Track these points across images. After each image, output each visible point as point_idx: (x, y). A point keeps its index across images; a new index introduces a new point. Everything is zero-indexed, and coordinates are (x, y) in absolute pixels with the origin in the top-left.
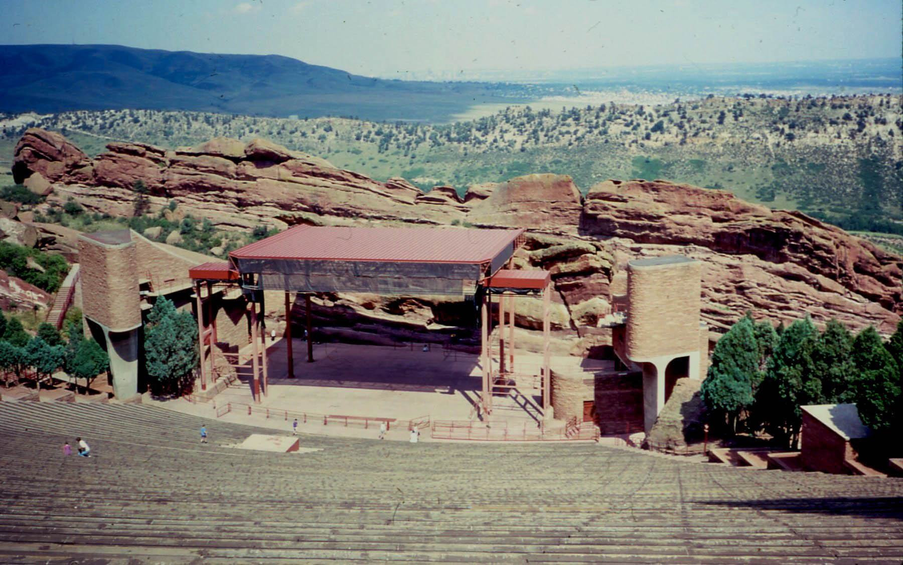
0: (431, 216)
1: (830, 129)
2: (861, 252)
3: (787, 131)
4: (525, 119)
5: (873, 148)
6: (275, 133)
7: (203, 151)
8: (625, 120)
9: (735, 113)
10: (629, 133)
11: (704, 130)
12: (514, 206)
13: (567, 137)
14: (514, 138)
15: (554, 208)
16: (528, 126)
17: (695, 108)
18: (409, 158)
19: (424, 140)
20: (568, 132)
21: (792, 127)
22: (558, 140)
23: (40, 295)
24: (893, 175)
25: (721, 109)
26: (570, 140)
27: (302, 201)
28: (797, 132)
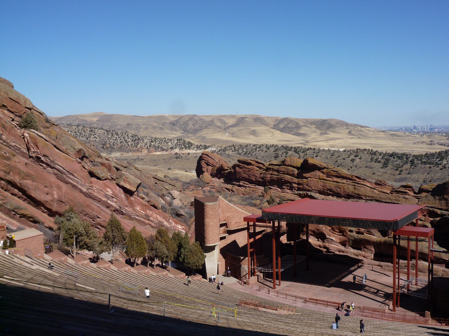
6: (329, 157)
18: (398, 172)
19: (407, 163)
23: (183, 227)
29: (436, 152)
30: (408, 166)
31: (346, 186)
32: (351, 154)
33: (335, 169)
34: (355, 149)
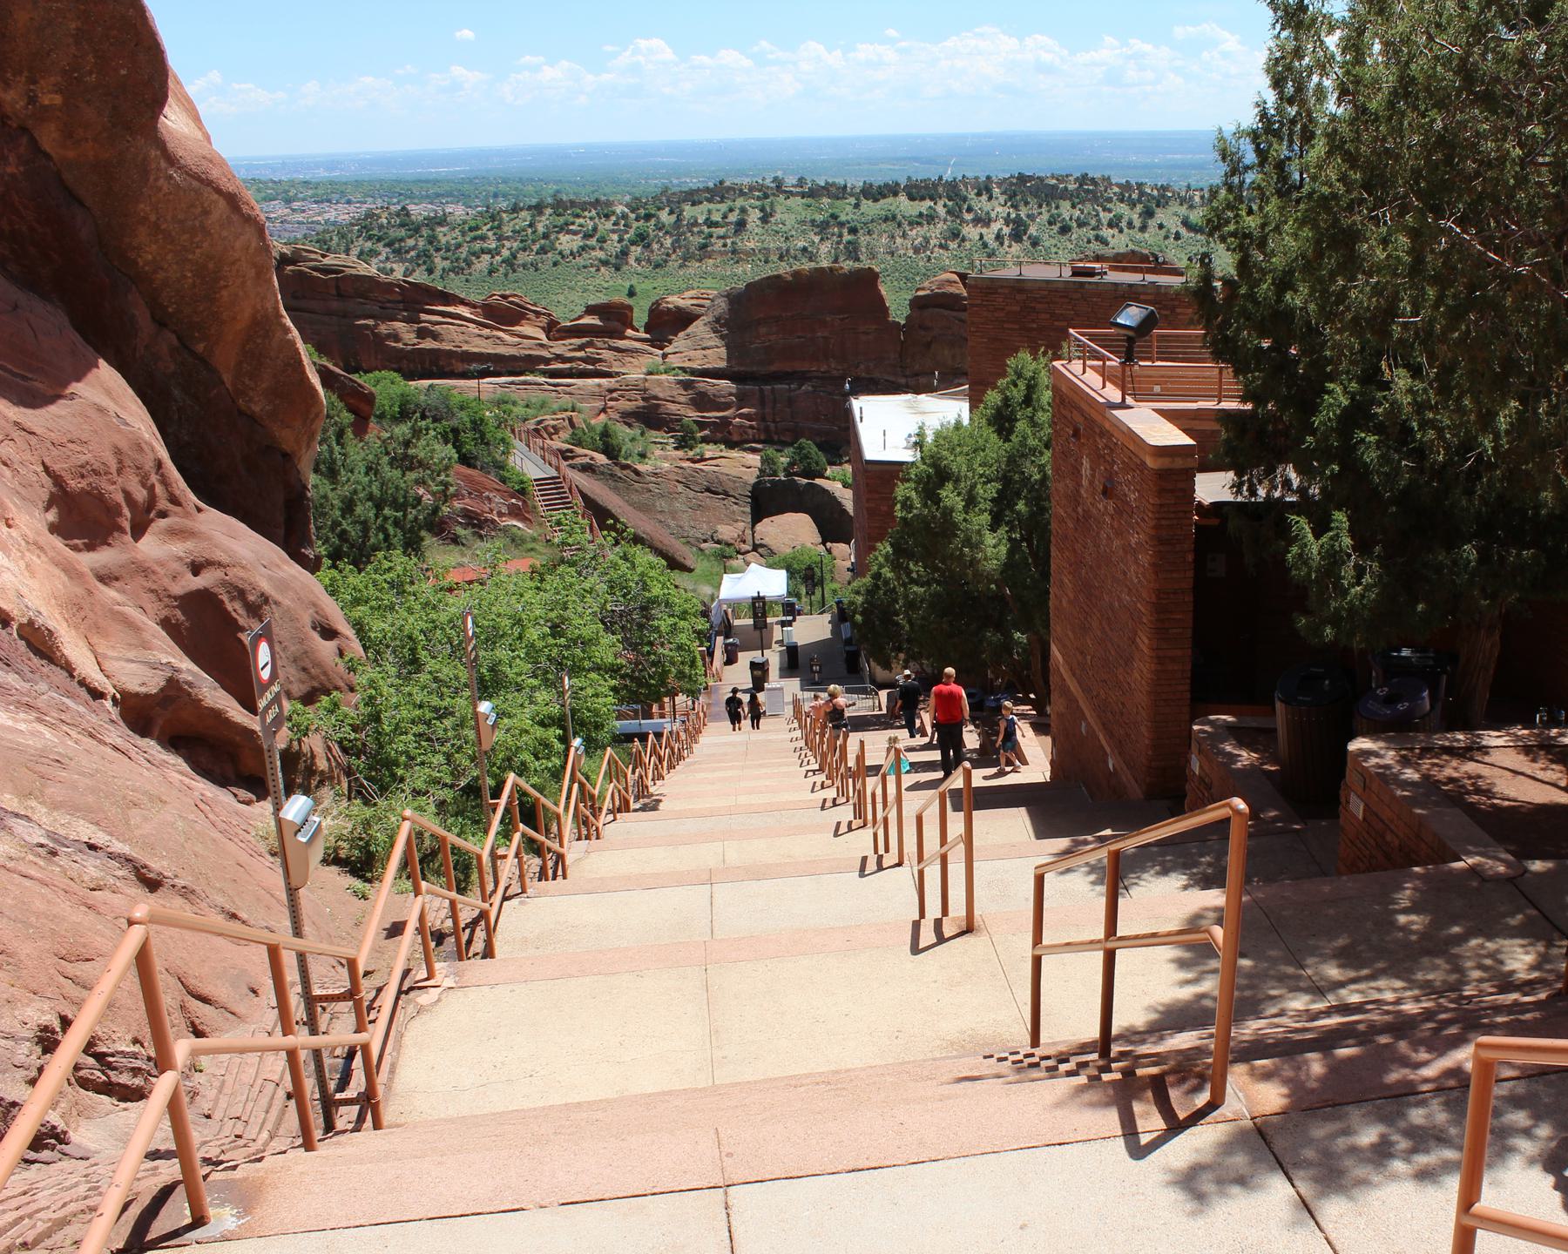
3: (847, 237)
4: (402, 233)
9: (762, 209)
14: (388, 266)
16: (411, 242)
20: (483, 251)
22: (469, 264)
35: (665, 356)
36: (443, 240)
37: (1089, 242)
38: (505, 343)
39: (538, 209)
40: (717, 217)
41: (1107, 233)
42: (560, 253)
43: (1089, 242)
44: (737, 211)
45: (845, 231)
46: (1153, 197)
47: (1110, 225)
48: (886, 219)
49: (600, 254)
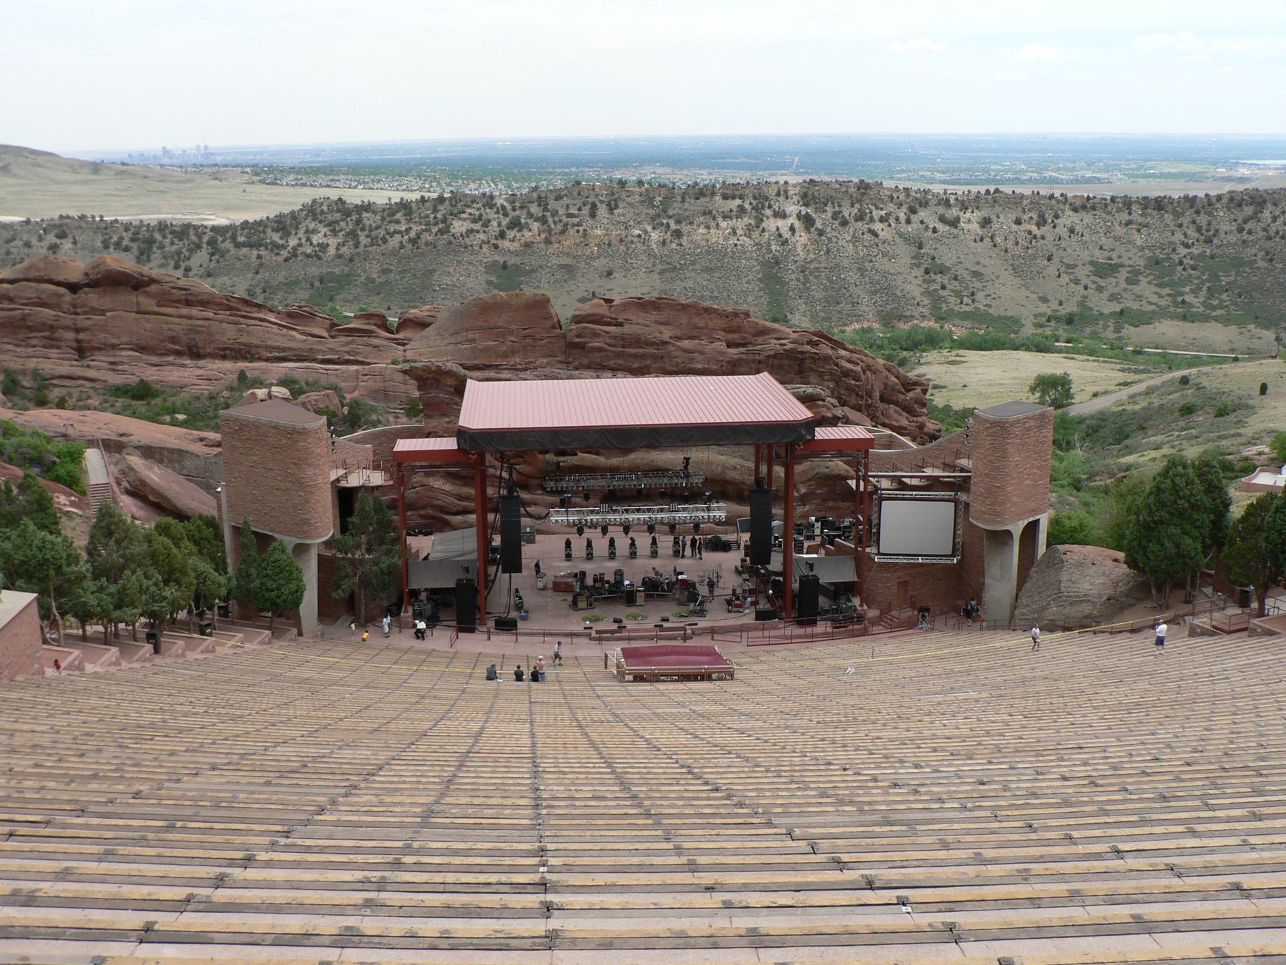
0: (358, 353)
1: (724, 224)
2: (886, 377)
3: (673, 226)
4: (338, 216)
5: (773, 247)
7: (21, 276)
8: (470, 214)
10: (478, 232)
11: (574, 225)
12: (471, 335)
13: (398, 237)
14: (325, 241)
15: (525, 337)
16: (343, 224)
17: (558, 198)
19: (199, 247)
21: (678, 222)
22: (385, 241)
23: (73, 498)
24: (798, 280)
25: (590, 200)
26: (401, 242)
27: (173, 340)
28: (685, 228)
29: (268, 218)
30: (202, 257)
31: (215, 327)
32: (45, 230)
33: (181, 283)
34: (56, 217)
35: (405, 351)
36: (367, 223)
37: (863, 234)
38: (296, 339)
39: (441, 199)
40: (574, 211)
41: (878, 226)
42: (453, 235)
43: (863, 234)
44: (589, 206)
45: (672, 222)
46: (916, 199)
47: (882, 220)
48: (704, 214)
49: (482, 236)
